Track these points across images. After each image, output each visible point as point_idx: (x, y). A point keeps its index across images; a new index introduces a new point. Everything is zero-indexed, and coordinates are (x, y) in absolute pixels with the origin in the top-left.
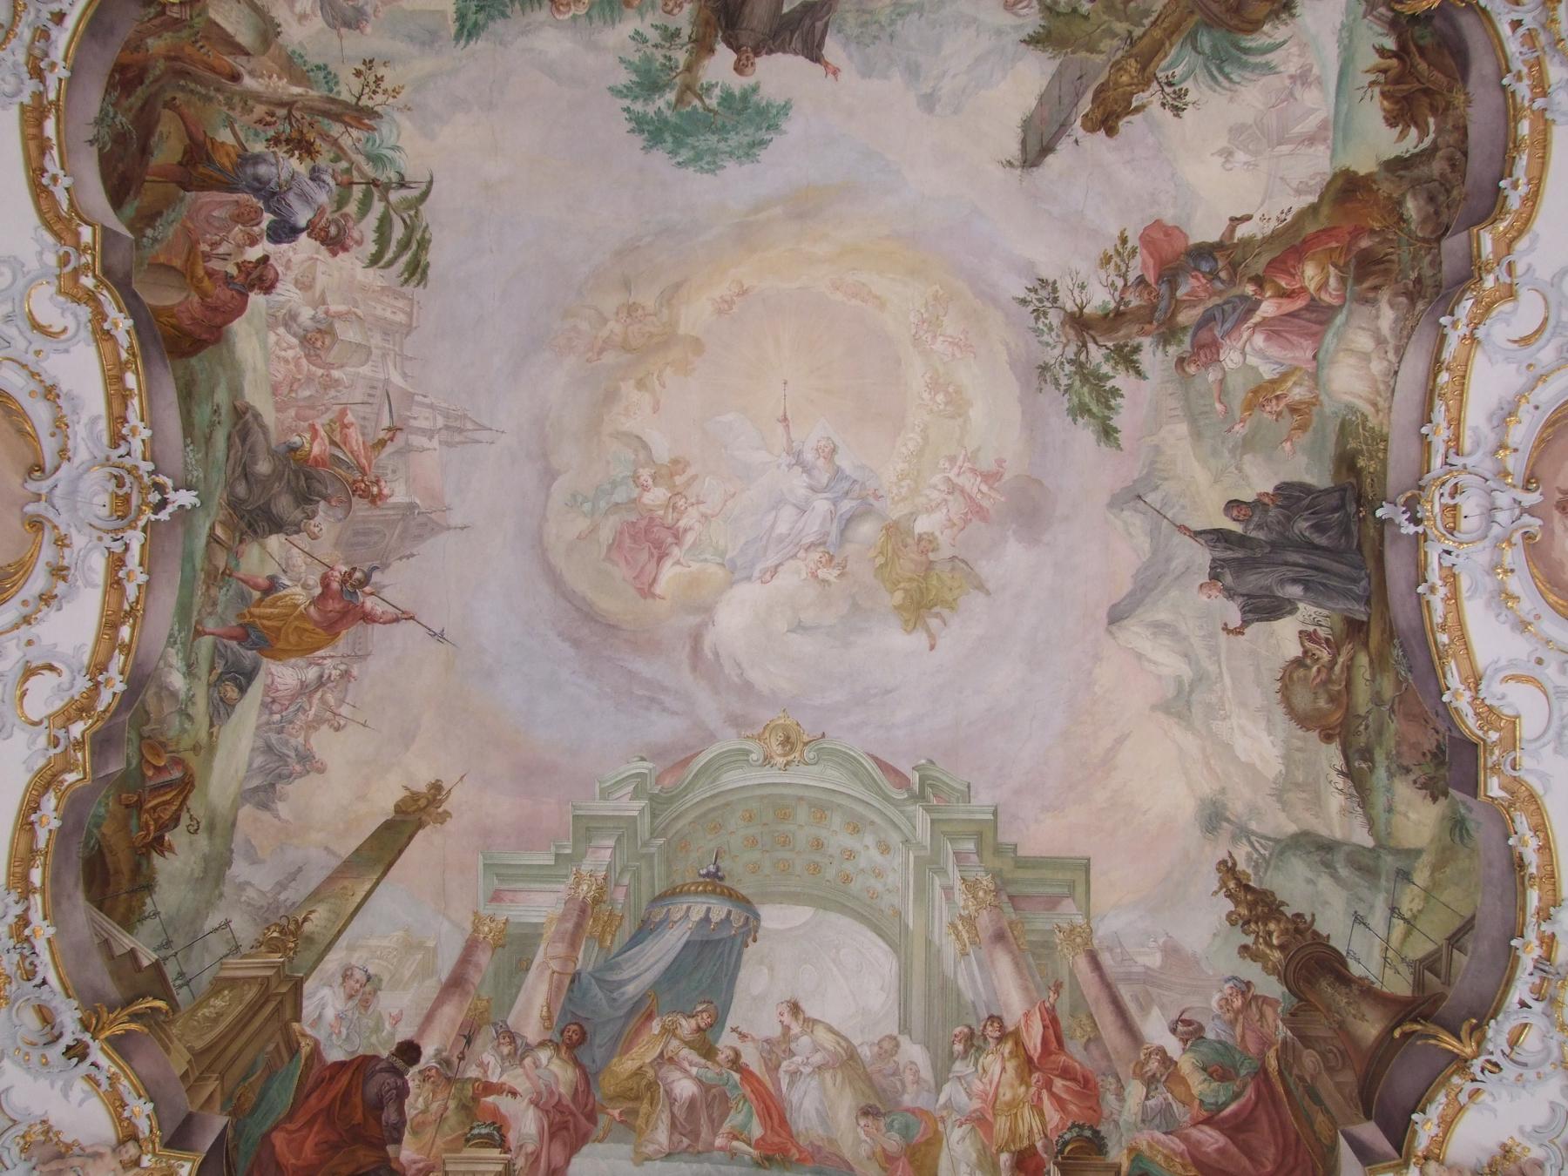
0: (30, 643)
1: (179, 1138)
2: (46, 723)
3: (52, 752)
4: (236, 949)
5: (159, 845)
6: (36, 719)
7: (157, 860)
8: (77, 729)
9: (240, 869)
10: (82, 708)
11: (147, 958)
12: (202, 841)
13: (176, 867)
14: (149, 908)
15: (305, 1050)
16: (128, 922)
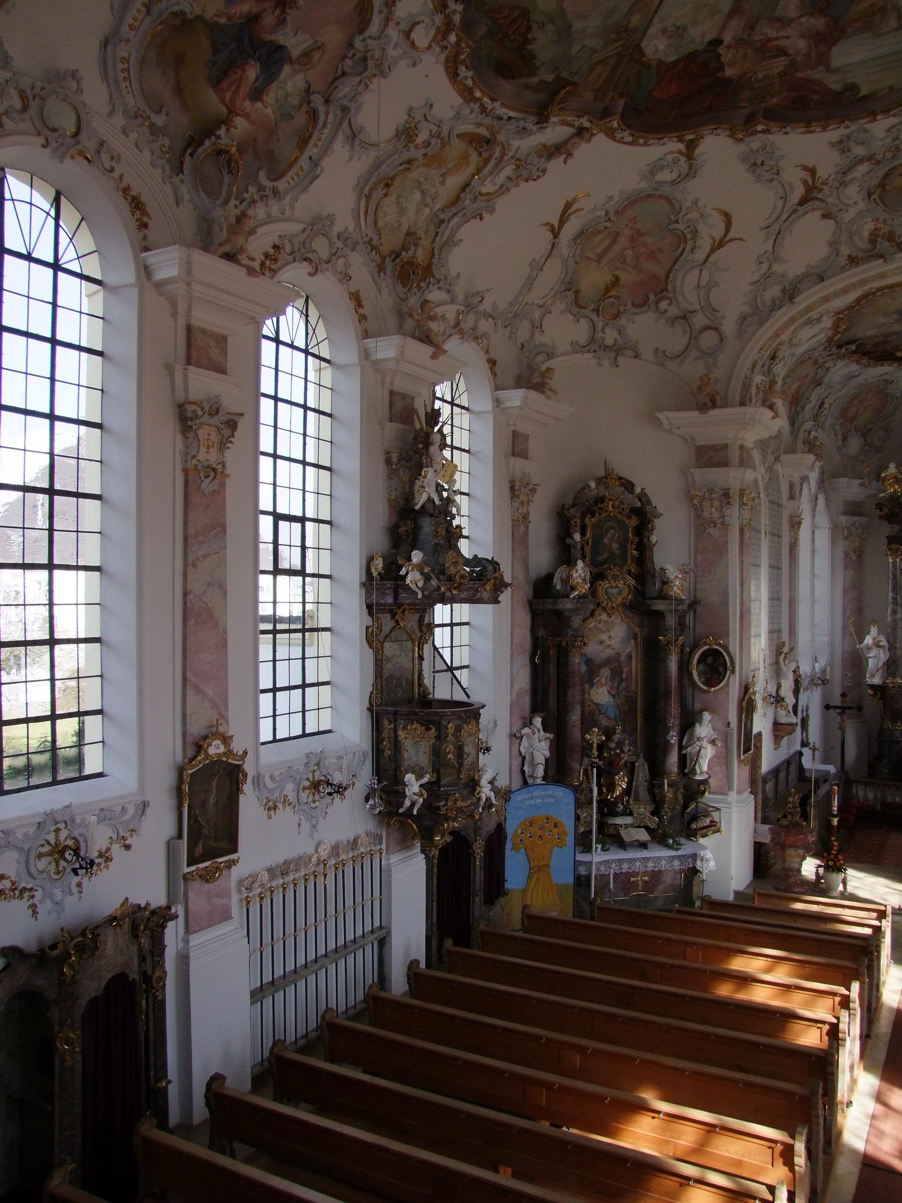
0: (397, 24)
1: (606, 114)
2: (433, 44)
3: (447, 52)
4: (595, 51)
5: (526, 41)
6: (426, 45)
7: (530, 47)
8: (453, 38)
9: (577, 25)
10: (448, 27)
11: (550, 78)
12: (550, 27)
13: (543, 44)
14: (538, 63)
15: (654, 64)
16: (532, 73)
